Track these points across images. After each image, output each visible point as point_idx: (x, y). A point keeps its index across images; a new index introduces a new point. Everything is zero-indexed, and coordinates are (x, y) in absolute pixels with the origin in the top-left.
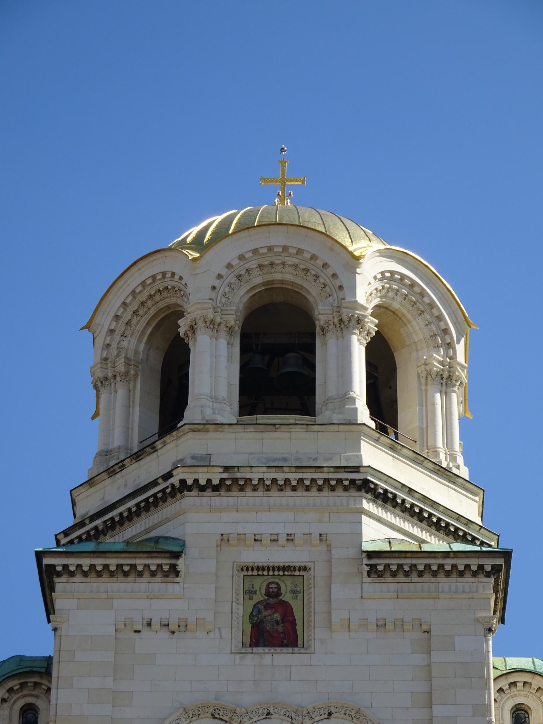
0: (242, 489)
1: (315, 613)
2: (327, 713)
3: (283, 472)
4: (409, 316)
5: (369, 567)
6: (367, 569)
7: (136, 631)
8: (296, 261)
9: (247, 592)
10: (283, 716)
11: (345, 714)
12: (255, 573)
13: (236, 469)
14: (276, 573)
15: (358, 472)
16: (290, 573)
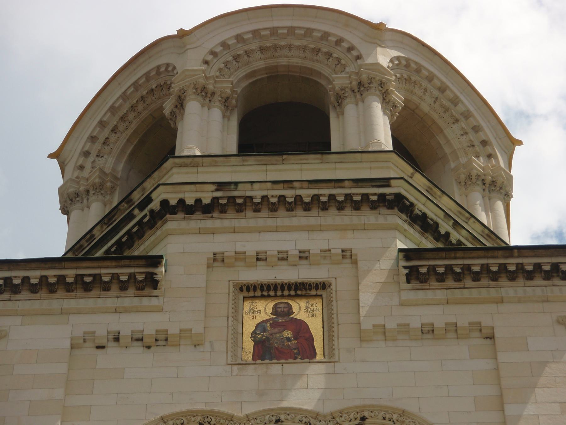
0: (240, 209)
1: (338, 324)
2: (359, 418)
3: (293, 188)
4: (440, 123)
5: (409, 270)
6: (406, 271)
7: (98, 347)
8: (304, 42)
9: (248, 312)
10: (299, 423)
11: (384, 419)
12: (259, 293)
13: (233, 187)
14: (286, 293)
15: (388, 186)
16: (304, 293)
